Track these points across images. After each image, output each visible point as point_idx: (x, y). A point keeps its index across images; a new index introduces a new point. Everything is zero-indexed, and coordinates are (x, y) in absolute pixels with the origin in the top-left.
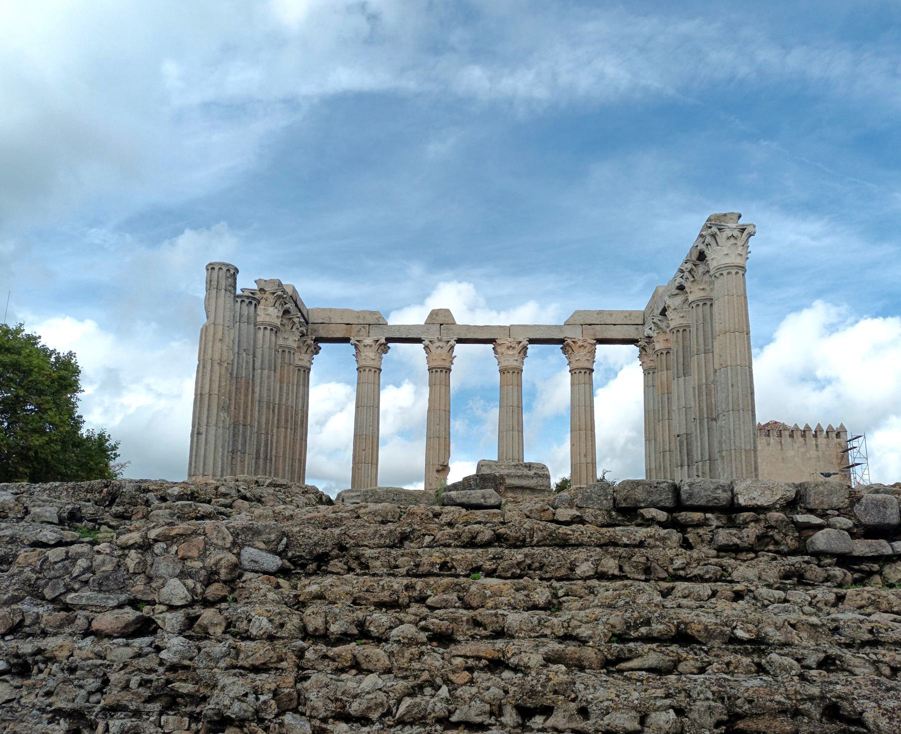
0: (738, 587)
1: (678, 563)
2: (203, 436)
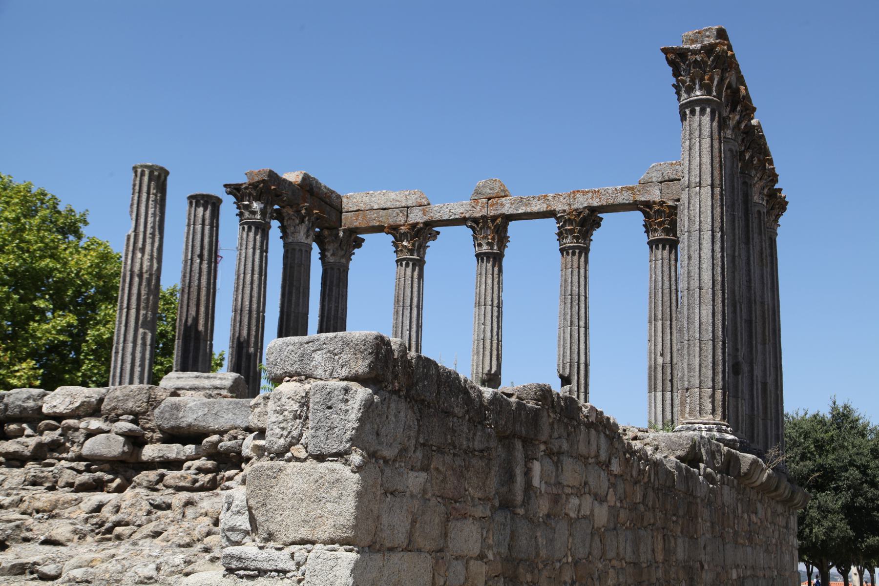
2: (120, 355)
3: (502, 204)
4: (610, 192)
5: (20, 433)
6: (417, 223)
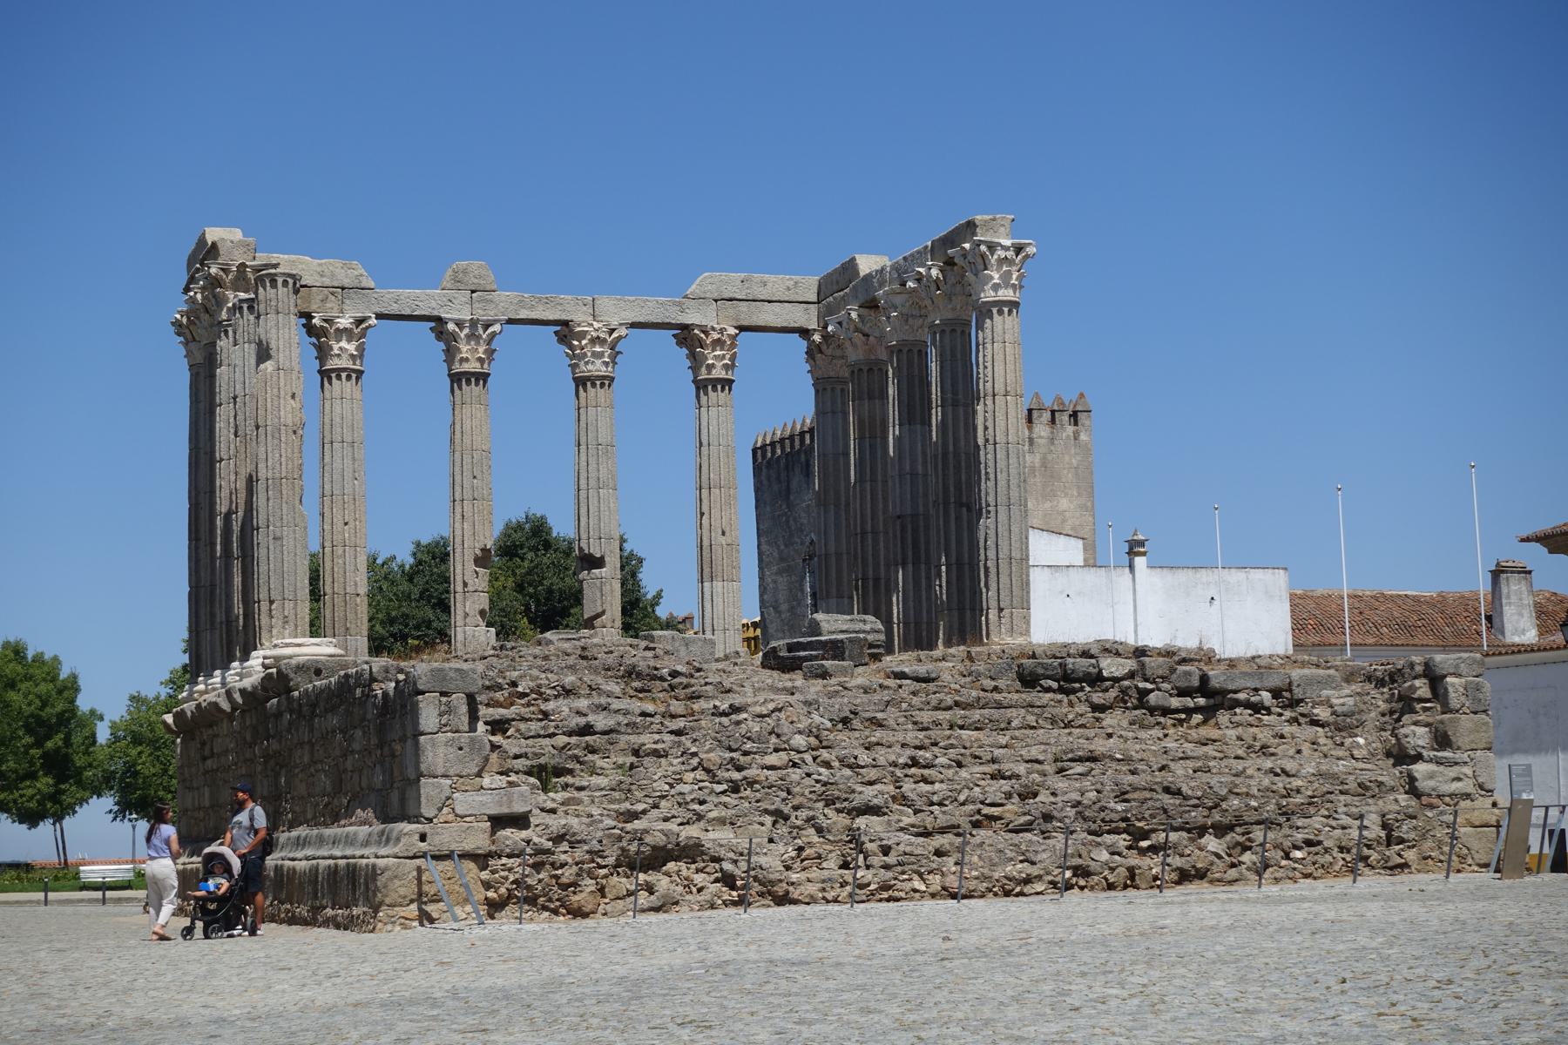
1: (1071, 717)
5: (1082, 689)
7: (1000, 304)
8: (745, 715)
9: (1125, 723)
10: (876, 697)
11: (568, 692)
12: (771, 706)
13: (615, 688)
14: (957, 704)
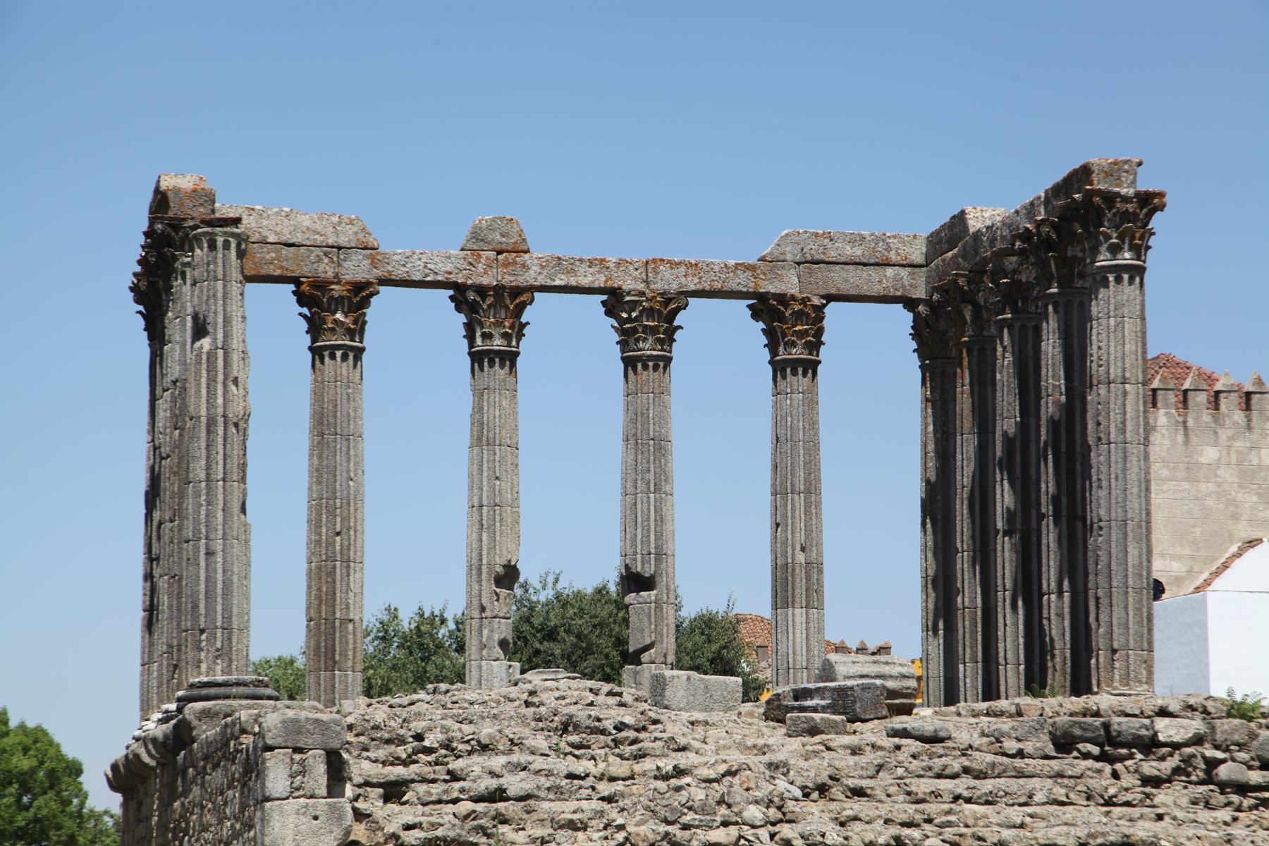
0: (1160, 811)
1: (1112, 791)
3: (524, 266)
4: (717, 268)
5: (1131, 756)
6: (368, 284)
7: (1118, 270)
8: (687, 780)
9: (1184, 802)
10: (862, 760)
11: (484, 748)
12: (722, 768)
13: (541, 742)
14: (966, 770)
